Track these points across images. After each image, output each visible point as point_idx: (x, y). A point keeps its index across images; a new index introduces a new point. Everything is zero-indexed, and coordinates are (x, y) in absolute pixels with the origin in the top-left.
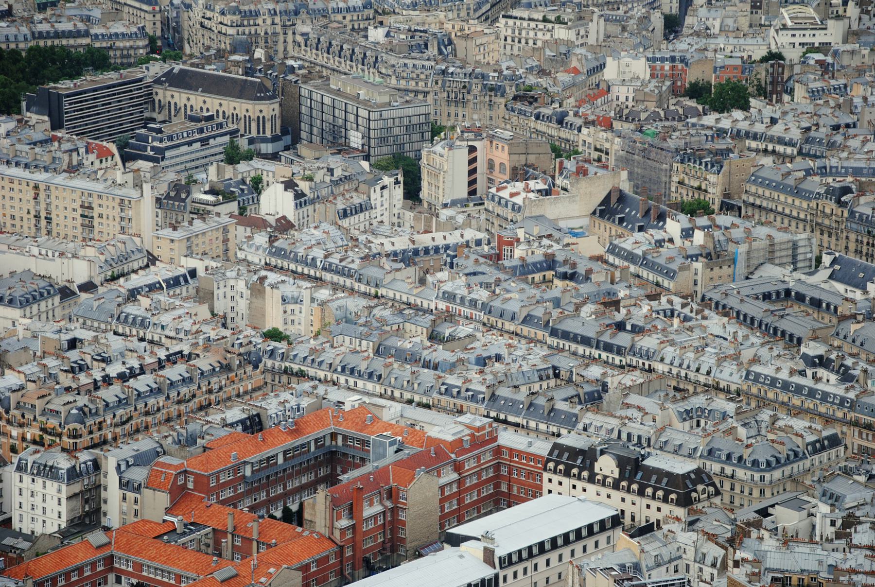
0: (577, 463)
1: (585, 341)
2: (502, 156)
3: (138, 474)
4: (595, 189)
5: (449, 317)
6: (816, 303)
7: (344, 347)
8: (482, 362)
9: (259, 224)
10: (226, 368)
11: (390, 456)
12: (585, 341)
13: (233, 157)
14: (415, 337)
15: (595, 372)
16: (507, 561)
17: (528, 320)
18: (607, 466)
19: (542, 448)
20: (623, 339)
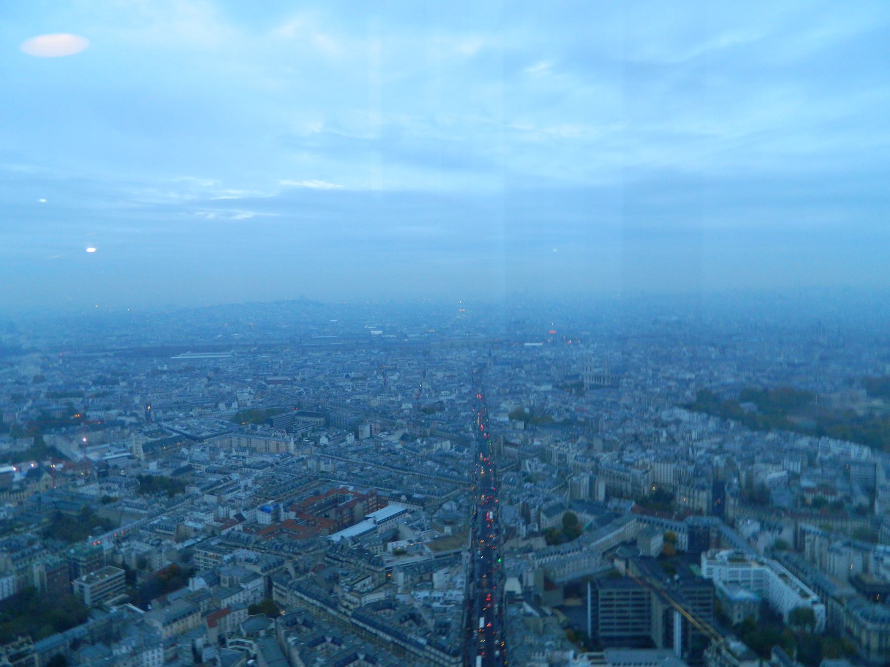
0: (396, 498)
1: (398, 469)
2: (378, 426)
3: (289, 508)
4: (400, 433)
5: (365, 465)
6: (452, 457)
7: (339, 473)
8: (374, 475)
9: (319, 446)
10: (310, 480)
11: (351, 499)
12: (398, 469)
13: (313, 431)
14: (357, 471)
15: (401, 476)
16: (379, 523)
17: (385, 465)
18: (403, 498)
19: (388, 494)
20: (408, 468)
